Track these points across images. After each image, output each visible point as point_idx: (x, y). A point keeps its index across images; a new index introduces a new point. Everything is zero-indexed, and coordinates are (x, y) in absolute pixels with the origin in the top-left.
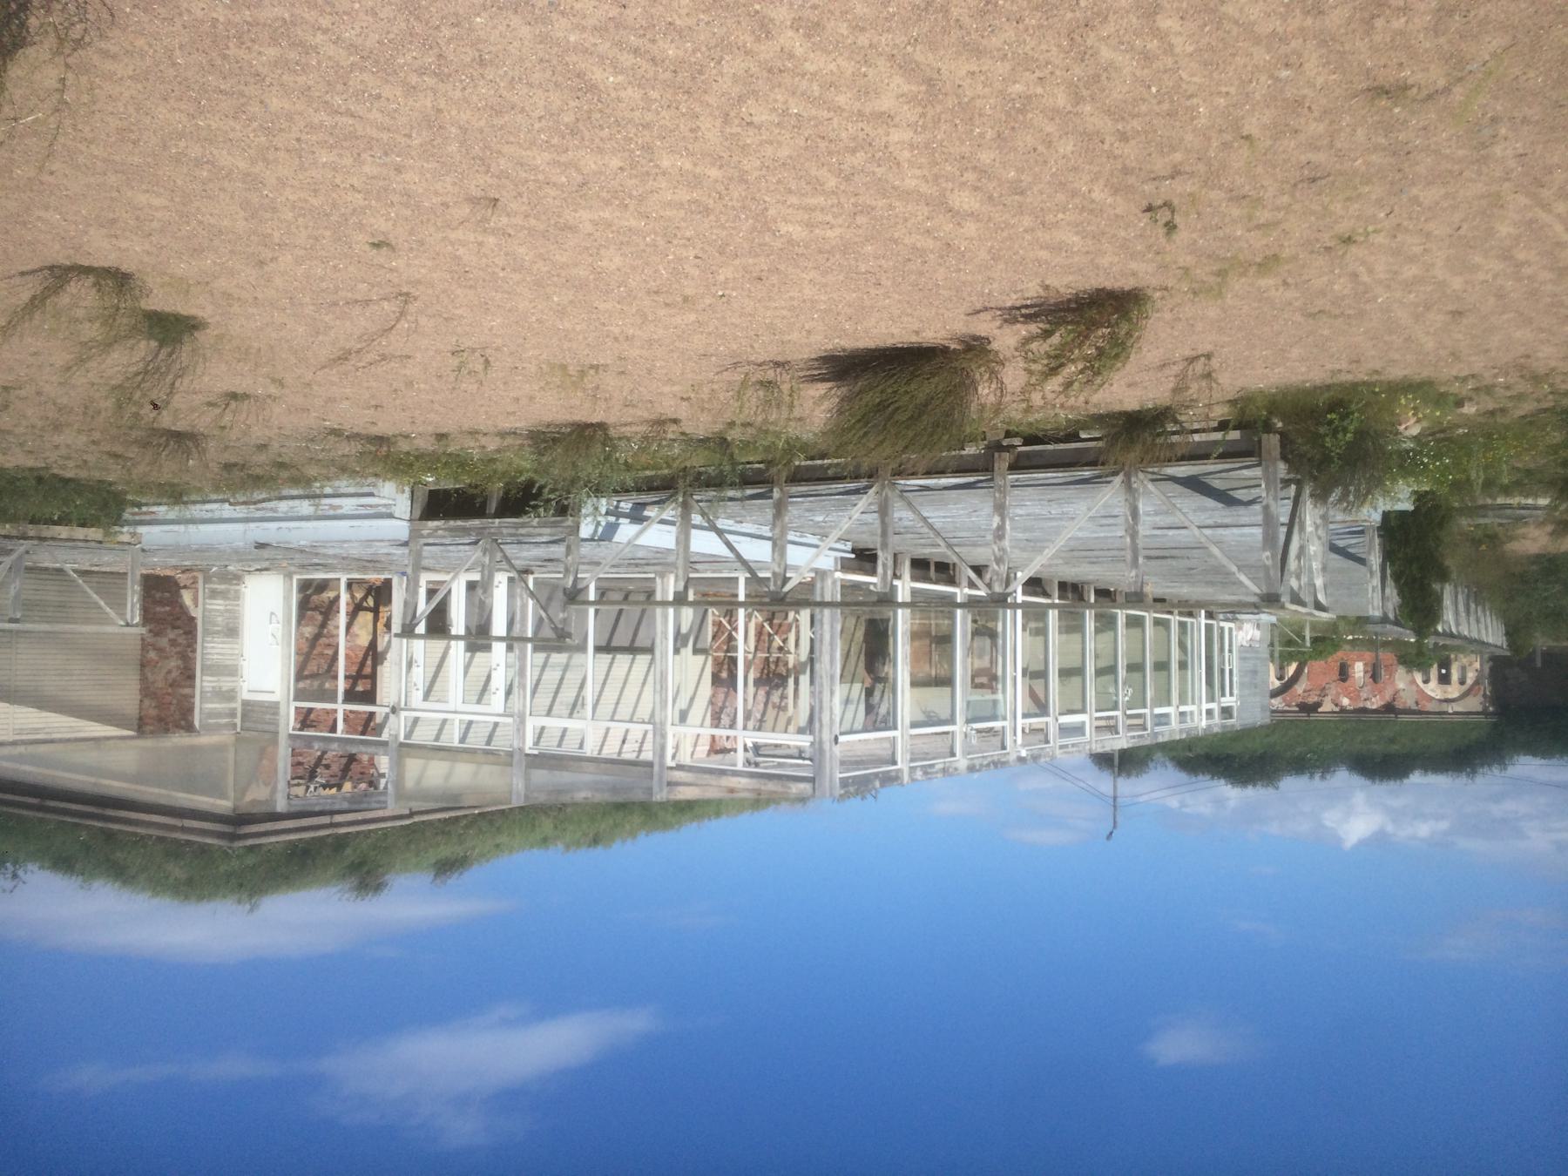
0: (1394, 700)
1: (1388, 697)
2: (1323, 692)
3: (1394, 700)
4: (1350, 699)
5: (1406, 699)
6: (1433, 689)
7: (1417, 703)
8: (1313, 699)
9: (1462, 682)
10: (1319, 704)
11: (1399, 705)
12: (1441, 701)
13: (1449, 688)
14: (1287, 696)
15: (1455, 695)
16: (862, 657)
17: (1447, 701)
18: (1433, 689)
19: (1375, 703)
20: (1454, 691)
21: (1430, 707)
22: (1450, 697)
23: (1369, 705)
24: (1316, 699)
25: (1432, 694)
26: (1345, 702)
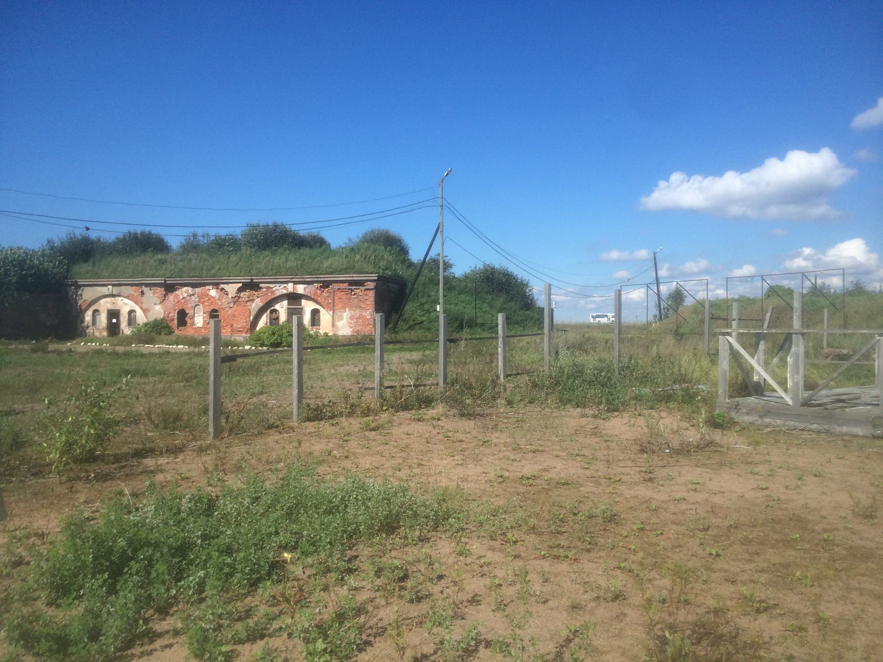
0: (165, 296)
1: (171, 297)
2: (236, 300)
3: (165, 296)
4: (207, 295)
5: (152, 296)
6: (125, 305)
7: (143, 293)
8: (244, 295)
9: (96, 312)
10: (240, 290)
11: (161, 291)
12: (119, 296)
13: (110, 307)
14: (270, 296)
15: (103, 301)
16: (407, 291)
17: (113, 296)
18: (125, 305)
19: (184, 292)
20: (105, 305)
21: (130, 290)
22: (108, 299)
23: (190, 290)
24: (242, 294)
25: (126, 301)
26: (213, 293)
